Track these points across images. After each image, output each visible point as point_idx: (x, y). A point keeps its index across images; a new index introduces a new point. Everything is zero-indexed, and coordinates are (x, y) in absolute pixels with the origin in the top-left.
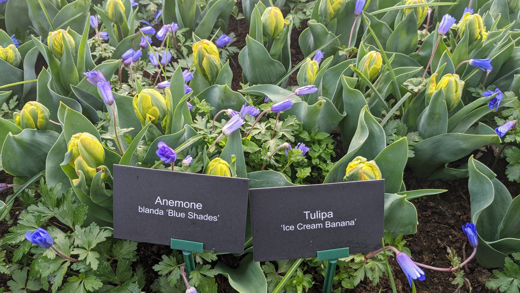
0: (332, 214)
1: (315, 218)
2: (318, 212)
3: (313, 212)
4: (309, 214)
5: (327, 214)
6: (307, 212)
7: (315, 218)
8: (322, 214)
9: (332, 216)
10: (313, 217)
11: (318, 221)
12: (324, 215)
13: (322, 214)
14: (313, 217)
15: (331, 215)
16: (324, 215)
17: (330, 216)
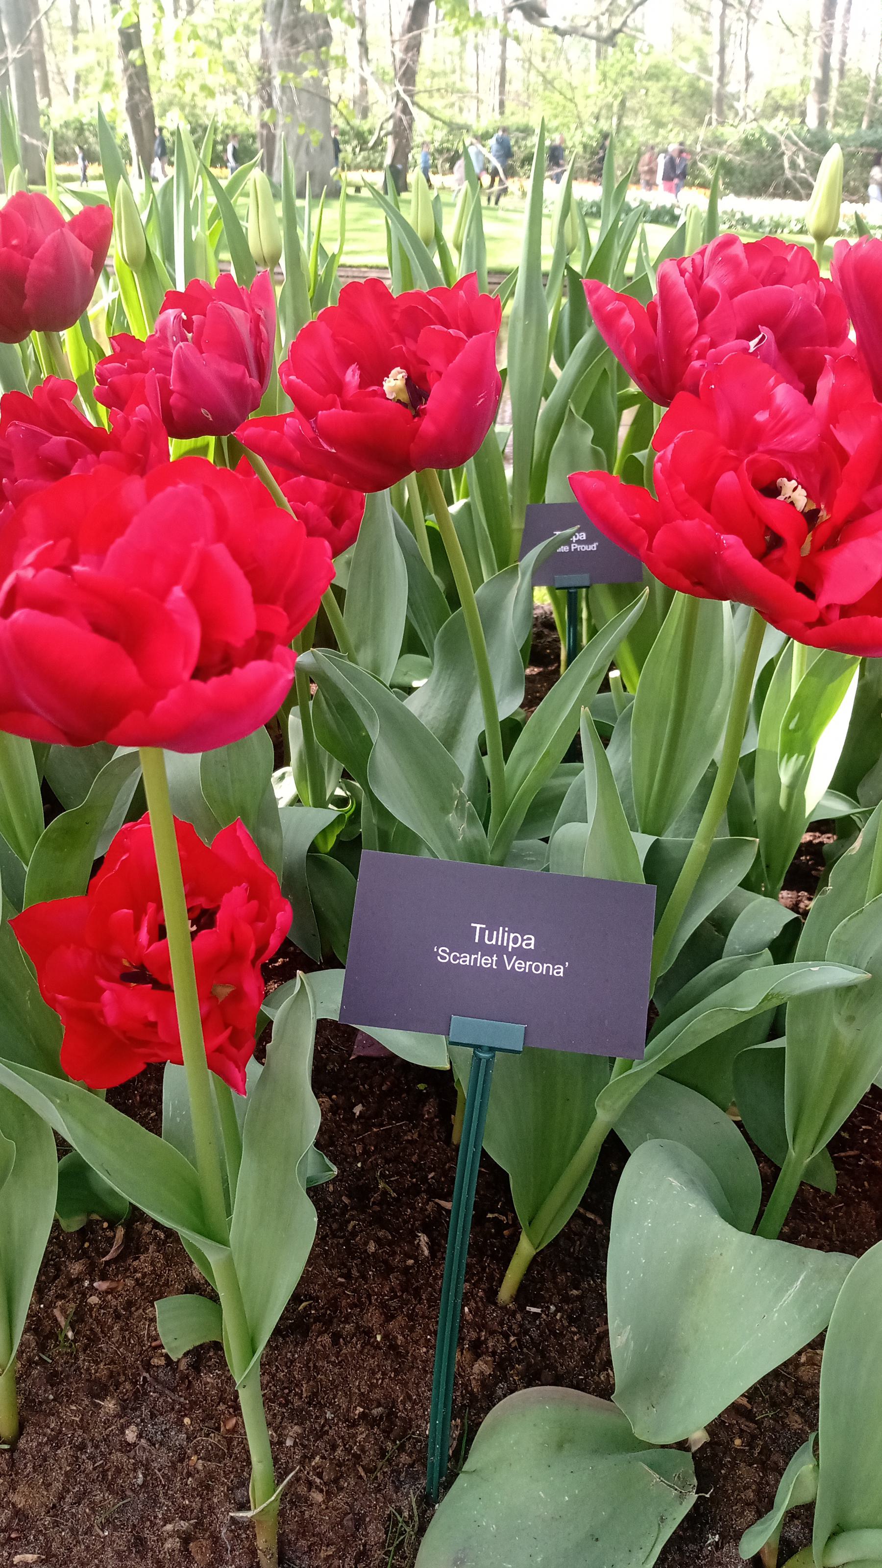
0: (533, 942)
1: (494, 942)
2: (504, 931)
3: (492, 928)
5: (523, 940)
6: (478, 926)
7: (494, 942)
8: (512, 935)
9: (532, 947)
10: (490, 939)
12: (515, 941)
13: (512, 935)
14: (490, 939)
15: (530, 942)
16: (515, 941)
17: (527, 945)
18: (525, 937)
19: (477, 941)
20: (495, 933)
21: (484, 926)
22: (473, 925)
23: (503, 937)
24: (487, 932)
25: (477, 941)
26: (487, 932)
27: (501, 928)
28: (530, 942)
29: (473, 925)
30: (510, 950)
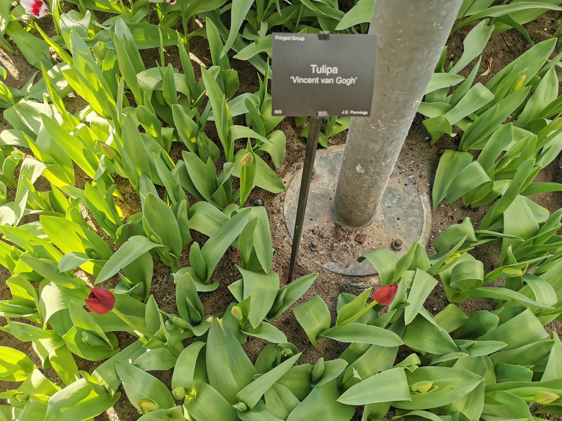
1: (320, 72)
3: (320, 66)
4: (316, 68)
6: (314, 66)
9: (337, 72)
10: (319, 71)
11: (323, 76)
12: (329, 70)
14: (319, 71)
15: (335, 70)
16: (329, 70)
18: (334, 68)
19: (313, 72)
20: (321, 68)
21: (316, 66)
22: (312, 66)
23: (325, 70)
24: (317, 69)
25: (313, 72)
26: (317, 69)
27: (323, 66)
28: (335, 70)
29: (312, 66)
30: (327, 75)
